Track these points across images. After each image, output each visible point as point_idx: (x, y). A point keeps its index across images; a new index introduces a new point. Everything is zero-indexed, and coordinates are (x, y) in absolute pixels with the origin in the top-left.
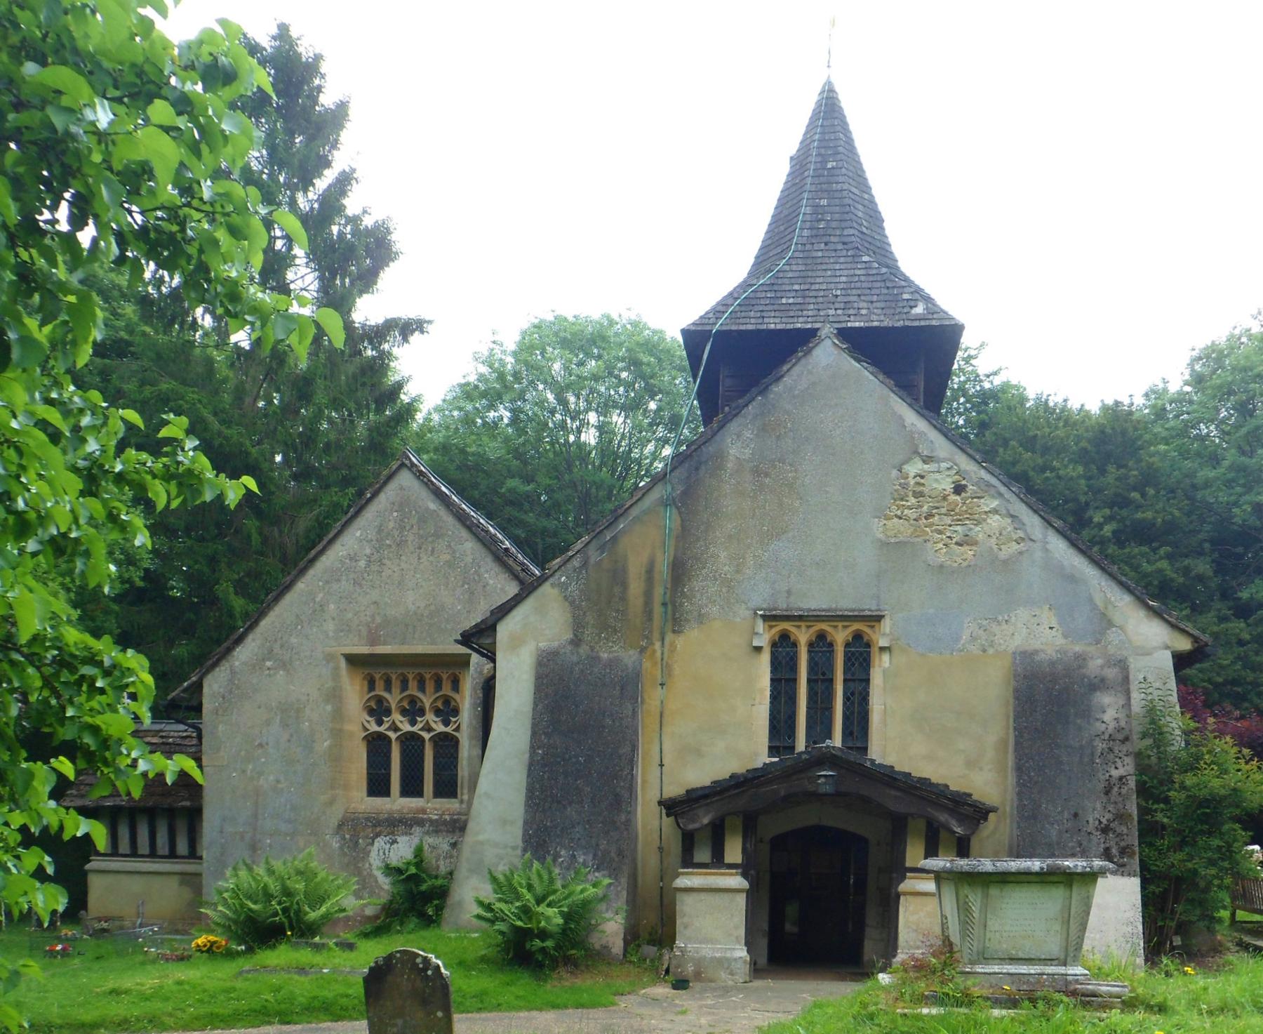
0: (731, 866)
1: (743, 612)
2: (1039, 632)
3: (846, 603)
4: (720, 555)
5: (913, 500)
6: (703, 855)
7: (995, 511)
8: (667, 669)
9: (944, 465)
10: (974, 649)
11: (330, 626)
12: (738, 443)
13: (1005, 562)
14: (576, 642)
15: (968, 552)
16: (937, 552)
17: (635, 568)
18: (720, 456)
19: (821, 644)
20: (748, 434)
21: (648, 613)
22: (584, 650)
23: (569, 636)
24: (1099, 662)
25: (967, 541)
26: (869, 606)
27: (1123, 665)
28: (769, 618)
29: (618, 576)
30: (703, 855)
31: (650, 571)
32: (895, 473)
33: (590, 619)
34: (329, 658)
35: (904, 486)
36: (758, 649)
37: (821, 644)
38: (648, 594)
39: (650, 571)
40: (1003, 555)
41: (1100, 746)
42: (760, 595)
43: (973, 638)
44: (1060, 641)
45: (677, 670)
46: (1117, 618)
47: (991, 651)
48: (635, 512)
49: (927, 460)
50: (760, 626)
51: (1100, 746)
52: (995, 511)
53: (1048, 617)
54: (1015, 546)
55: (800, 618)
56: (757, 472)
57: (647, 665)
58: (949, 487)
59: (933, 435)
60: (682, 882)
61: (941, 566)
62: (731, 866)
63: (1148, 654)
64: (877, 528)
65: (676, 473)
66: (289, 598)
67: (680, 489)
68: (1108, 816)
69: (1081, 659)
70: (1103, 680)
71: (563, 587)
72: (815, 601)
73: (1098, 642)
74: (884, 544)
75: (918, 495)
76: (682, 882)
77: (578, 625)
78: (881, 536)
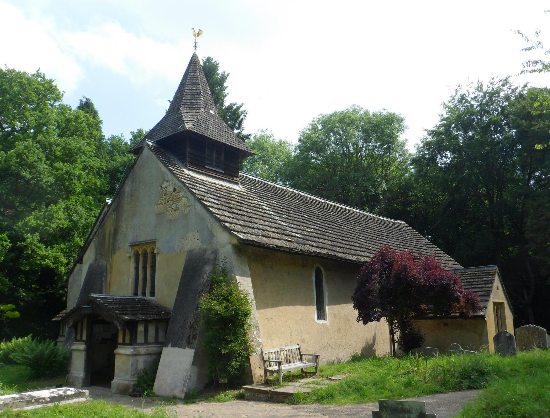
0: (84, 341)
1: (127, 245)
2: (193, 242)
5: (164, 196)
7: (183, 196)
8: (111, 267)
9: (171, 182)
14: (96, 260)
15: (177, 213)
17: (107, 233)
19: (145, 254)
21: (109, 248)
24: (210, 252)
25: (177, 209)
27: (216, 252)
29: (104, 236)
32: (160, 188)
37: (145, 254)
38: (109, 241)
39: (110, 234)
40: (186, 212)
41: (200, 289)
42: (130, 239)
43: (178, 246)
44: (200, 244)
46: (215, 234)
47: (182, 251)
48: (108, 215)
49: (167, 181)
51: (200, 289)
52: (183, 196)
54: (188, 209)
55: (138, 245)
56: (132, 195)
57: (108, 266)
58: (172, 190)
59: (168, 173)
60: (73, 347)
61: (170, 220)
63: (224, 247)
65: (116, 199)
67: (116, 204)
68: (194, 320)
69: (205, 251)
70: (209, 259)
71: (94, 241)
72: (142, 239)
73: (211, 243)
75: (166, 194)
76: (73, 347)
78: (157, 211)
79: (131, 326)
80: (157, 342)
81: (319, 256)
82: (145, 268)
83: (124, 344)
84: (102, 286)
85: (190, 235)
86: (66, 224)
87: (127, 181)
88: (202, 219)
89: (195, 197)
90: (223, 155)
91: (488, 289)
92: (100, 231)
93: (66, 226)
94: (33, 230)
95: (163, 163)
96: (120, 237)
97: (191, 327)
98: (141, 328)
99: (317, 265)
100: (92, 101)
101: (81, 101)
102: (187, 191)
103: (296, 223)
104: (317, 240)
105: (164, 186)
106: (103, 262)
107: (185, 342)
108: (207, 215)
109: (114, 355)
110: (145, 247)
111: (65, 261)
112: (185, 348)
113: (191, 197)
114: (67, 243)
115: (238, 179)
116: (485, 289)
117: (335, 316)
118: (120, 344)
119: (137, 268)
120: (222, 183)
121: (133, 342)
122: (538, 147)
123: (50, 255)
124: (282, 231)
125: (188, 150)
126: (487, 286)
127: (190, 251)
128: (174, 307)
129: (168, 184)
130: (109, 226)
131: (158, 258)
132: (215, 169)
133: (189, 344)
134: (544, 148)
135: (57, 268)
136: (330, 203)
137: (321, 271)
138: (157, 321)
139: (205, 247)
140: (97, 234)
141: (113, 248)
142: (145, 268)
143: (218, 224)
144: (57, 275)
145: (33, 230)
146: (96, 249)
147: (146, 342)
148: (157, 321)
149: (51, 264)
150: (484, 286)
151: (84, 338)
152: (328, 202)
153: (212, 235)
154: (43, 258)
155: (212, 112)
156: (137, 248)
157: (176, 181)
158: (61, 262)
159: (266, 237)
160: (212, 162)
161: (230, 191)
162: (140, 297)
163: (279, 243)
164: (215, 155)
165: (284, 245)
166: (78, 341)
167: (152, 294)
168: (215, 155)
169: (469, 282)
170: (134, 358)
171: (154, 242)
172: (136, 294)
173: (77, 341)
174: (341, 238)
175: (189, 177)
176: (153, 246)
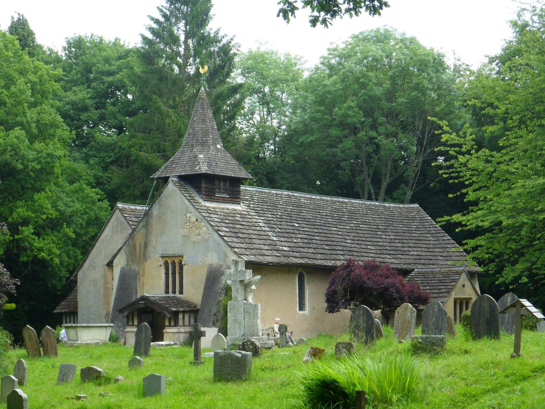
0: (136, 326)
1: (158, 256)
2: (213, 259)
3: (177, 252)
4: (153, 241)
5: (188, 224)
6: (130, 323)
7: (204, 226)
10: (201, 264)
11: (103, 256)
12: (155, 211)
13: (206, 240)
14: (127, 265)
15: (199, 237)
16: (194, 238)
18: (152, 213)
19: (173, 263)
20: (157, 208)
21: (140, 256)
22: (129, 267)
23: (126, 263)
25: (199, 234)
28: (162, 257)
29: (134, 247)
30: (130, 323)
31: (140, 245)
33: (130, 259)
34: (103, 265)
35: (187, 220)
36: (161, 265)
37: (173, 263)
38: (140, 251)
39: (140, 245)
40: (206, 238)
42: (160, 251)
43: (201, 261)
45: (146, 272)
46: (228, 255)
48: (137, 229)
49: (191, 213)
50: (161, 259)
51: (219, 291)
52: (204, 226)
53: (215, 255)
54: (208, 235)
55: (168, 257)
56: (159, 218)
57: (140, 270)
58: (195, 220)
59: (191, 206)
62: (136, 326)
64: (182, 232)
66: (95, 248)
69: (221, 266)
71: (125, 250)
72: (171, 252)
74: (183, 236)
75: (189, 222)
76: (127, 330)
77: (128, 260)
79: (176, 314)
80: (190, 325)
82: (174, 274)
83: (170, 326)
84: (137, 286)
85: (210, 254)
86: (54, 214)
87: (154, 206)
88: (219, 244)
89: (213, 228)
90: (228, 183)
91: (451, 287)
92: (130, 241)
93: (54, 216)
94: (25, 222)
95: (187, 198)
96: (150, 249)
97: (215, 315)
98: (181, 316)
99: (300, 270)
100: (26, 17)
101: (13, 18)
102: (207, 223)
103: (286, 235)
104: (301, 249)
105: (188, 215)
106: (135, 267)
107: (211, 323)
108: (222, 242)
109: (163, 333)
110: (173, 259)
111: (58, 252)
112: (211, 327)
113: (210, 228)
114: (56, 234)
115: (239, 200)
116: (449, 287)
117: (314, 308)
118: (167, 326)
119: (167, 274)
122: (450, 196)
123: (48, 247)
124: (274, 247)
125: (204, 185)
126: (451, 284)
127: (210, 266)
128: (202, 302)
129: (191, 215)
130: (139, 238)
131: (185, 268)
132: (222, 196)
133: (214, 325)
134: (454, 197)
135: (52, 259)
136: (326, 198)
137: (303, 275)
138: (190, 312)
139: (221, 263)
140: (127, 243)
141: (145, 257)
142: (174, 274)
143: (230, 249)
144: (51, 266)
145: (25, 222)
146: (127, 255)
147: (184, 325)
148: (190, 312)
149: (46, 256)
150: (448, 284)
151: (136, 323)
152: (323, 198)
153: (226, 256)
154: (40, 250)
155: (218, 146)
156: (166, 259)
157: (198, 214)
158: (54, 253)
159: (262, 255)
160: (220, 190)
161: (234, 213)
162: (171, 295)
163: (269, 259)
164: (222, 185)
165: (274, 261)
166: (131, 326)
167: (181, 292)
168: (222, 185)
169: (440, 280)
170: (178, 334)
171: (183, 256)
172: (167, 292)
173: (128, 325)
174: (325, 243)
175: (205, 208)
176: (180, 258)
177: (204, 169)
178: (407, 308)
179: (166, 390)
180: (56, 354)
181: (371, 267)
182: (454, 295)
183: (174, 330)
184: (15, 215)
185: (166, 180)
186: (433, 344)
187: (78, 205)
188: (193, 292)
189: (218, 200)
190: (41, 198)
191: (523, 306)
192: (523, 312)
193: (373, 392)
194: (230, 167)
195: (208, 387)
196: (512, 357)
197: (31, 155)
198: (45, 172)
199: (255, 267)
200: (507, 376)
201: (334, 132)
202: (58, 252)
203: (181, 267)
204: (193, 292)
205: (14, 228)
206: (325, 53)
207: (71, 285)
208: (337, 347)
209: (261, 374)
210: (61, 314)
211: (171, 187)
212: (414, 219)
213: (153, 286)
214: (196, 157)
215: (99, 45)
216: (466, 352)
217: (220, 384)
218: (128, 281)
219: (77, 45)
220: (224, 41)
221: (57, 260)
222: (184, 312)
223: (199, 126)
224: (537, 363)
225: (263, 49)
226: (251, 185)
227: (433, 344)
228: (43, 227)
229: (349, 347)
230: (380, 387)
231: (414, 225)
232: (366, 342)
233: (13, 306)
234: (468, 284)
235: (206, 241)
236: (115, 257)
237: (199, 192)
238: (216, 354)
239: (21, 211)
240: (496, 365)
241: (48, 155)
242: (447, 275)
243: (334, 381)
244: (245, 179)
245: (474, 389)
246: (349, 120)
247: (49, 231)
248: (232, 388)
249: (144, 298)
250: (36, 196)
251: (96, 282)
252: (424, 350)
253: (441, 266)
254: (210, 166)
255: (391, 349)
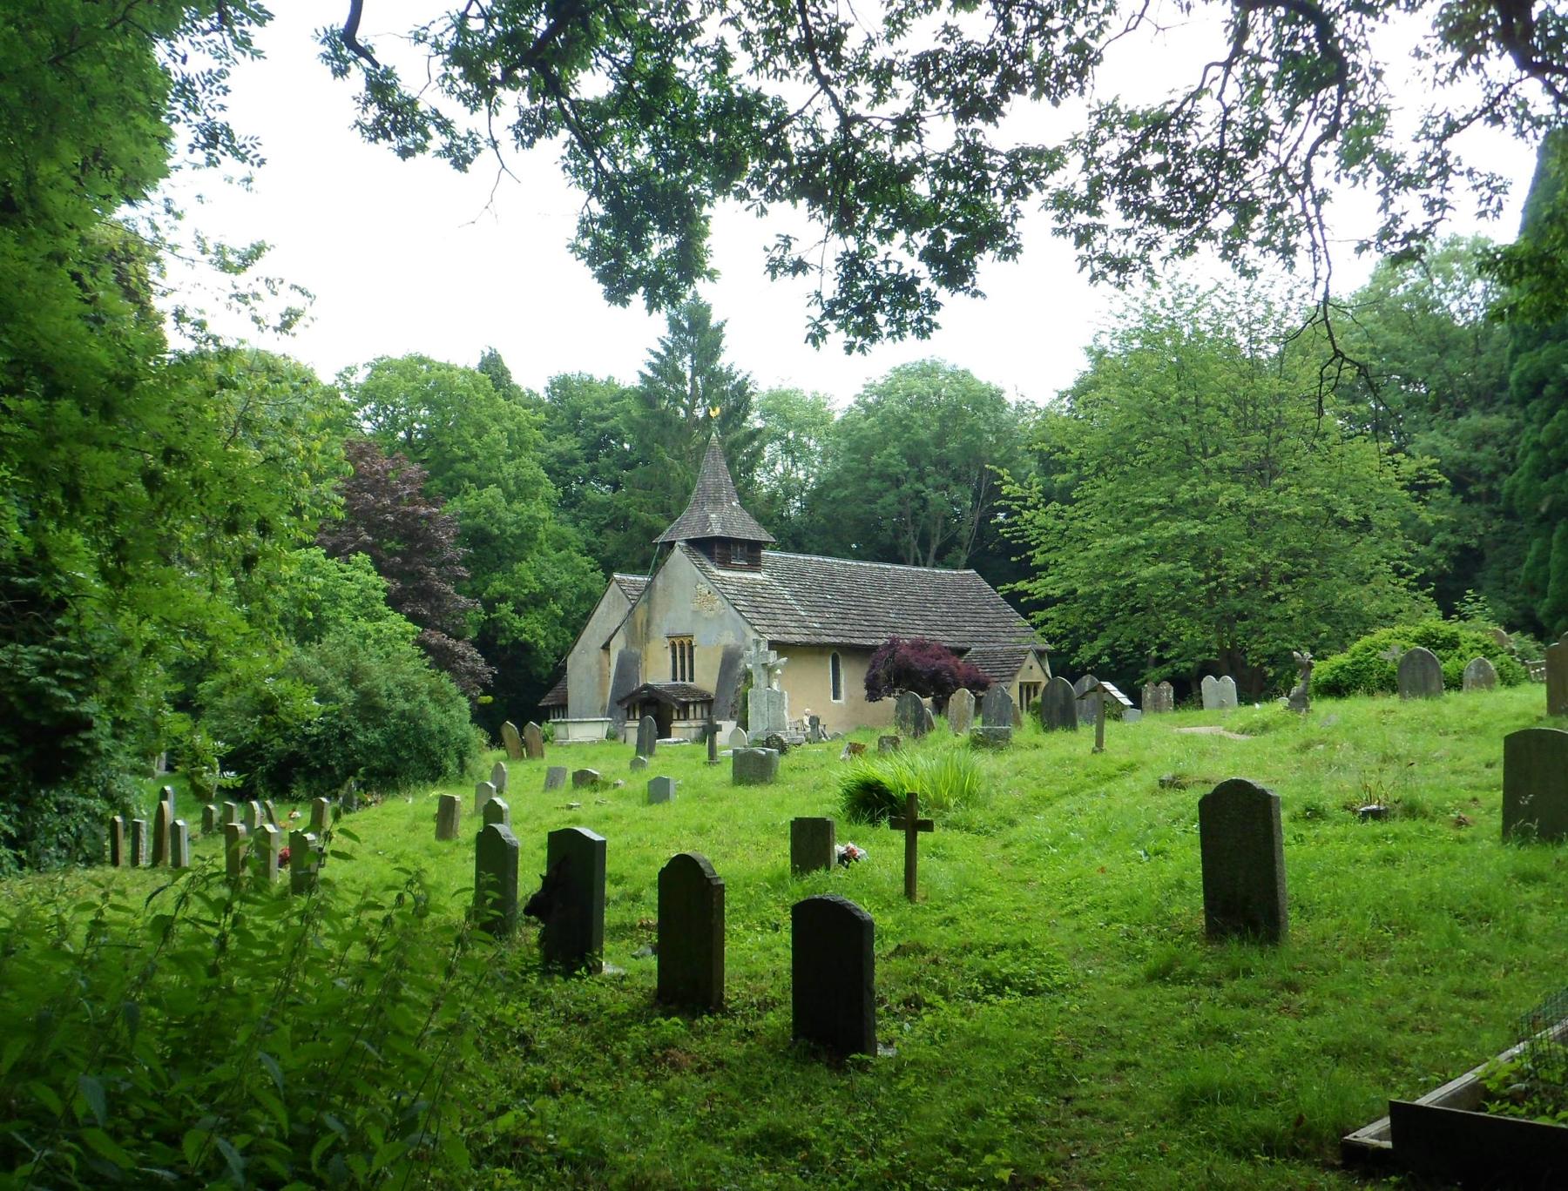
1: (663, 636)
2: (729, 639)
3: (684, 632)
4: (657, 618)
16: (706, 614)
19: (682, 644)
26: (690, 632)
37: (682, 644)
79: (685, 705)
81: (834, 645)
82: (682, 657)
86: (538, 587)
94: (503, 598)
96: (653, 627)
106: (635, 650)
111: (543, 633)
119: (674, 657)
120: (746, 575)
121: (686, 718)
123: (532, 628)
127: (726, 646)
130: (641, 614)
133: (732, 718)
138: (702, 702)
141: (647, 637)
142: (682, 657)
145: (503, 598)
148: (702, 702)
154: (522, 631)
161: (755, 583)
163: (797, 638)
167: (691, 679)
172: (675, 679)
177: (717, 531)
178: (963, 694)
179: (676, 797)
180: (542, 755)
181: (920, 646)
182: (1019, 679)
183: (684, 724)
184: (490, 590)
185: (671, 545)
186: (996, 737)
187: (566, 577)
188: (706, 678)
189: (733, 569)
190: (521, 569)
191: (1105, 690)
192: (1106, 697)
193: (926, 795)
194: (747, 529)
195: (726, 791)
196: (1094, 752)
197: (510, 517)
198: (527, 537)
199: (779, 647)
200: (1088, 776)
201: (873, 484)
202: (543, 633)
203: (691, 648)
204: (706, 678)
205: (489, 606)
206: (861, 391)
207: (560, 673)
208: (880, 741)
209: (789, 775)
210: (547, 708)
211: (678, 553)
212: (970, 588)
213: (658, 672)
214: (707, 517)
215: (588, 384)
216: (1037, 746)
217: (740, 788)
218: (628, 666)
219: (562, 386)
220: (739, 378)
221: (542, 643)
222: (695, 703)
223: (710, 481)
224: (1125, 760)
225: (785, 388)
226: (772, 549)
227: (996, 737)
228: (524, 604)
229: (895, 741)
230: (935, 790)
231: (970, 595)
232: (915, 735)
233: (489, 699)
234: (1036, 665)
235: (721, 617)
236: (611, 638)
237: (712, 559)
238: (735, 752)
239: (498, 585)
240: (1074, 761)
241: (530, 517)
242: (1011, 654)
243: (879, 782)
244: (766, 543)
245: (1049, 791)
246: (891, 470)
247: (531, 608)
248: (755, 793)
249: (646, 687)
250: (516, 567)
251: (589, 670)
252: (986, 744)
253: (1004, 644)
254: (723, 527)
255: (945, 744)
